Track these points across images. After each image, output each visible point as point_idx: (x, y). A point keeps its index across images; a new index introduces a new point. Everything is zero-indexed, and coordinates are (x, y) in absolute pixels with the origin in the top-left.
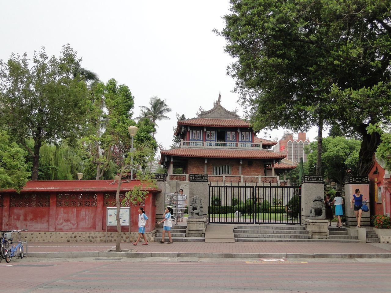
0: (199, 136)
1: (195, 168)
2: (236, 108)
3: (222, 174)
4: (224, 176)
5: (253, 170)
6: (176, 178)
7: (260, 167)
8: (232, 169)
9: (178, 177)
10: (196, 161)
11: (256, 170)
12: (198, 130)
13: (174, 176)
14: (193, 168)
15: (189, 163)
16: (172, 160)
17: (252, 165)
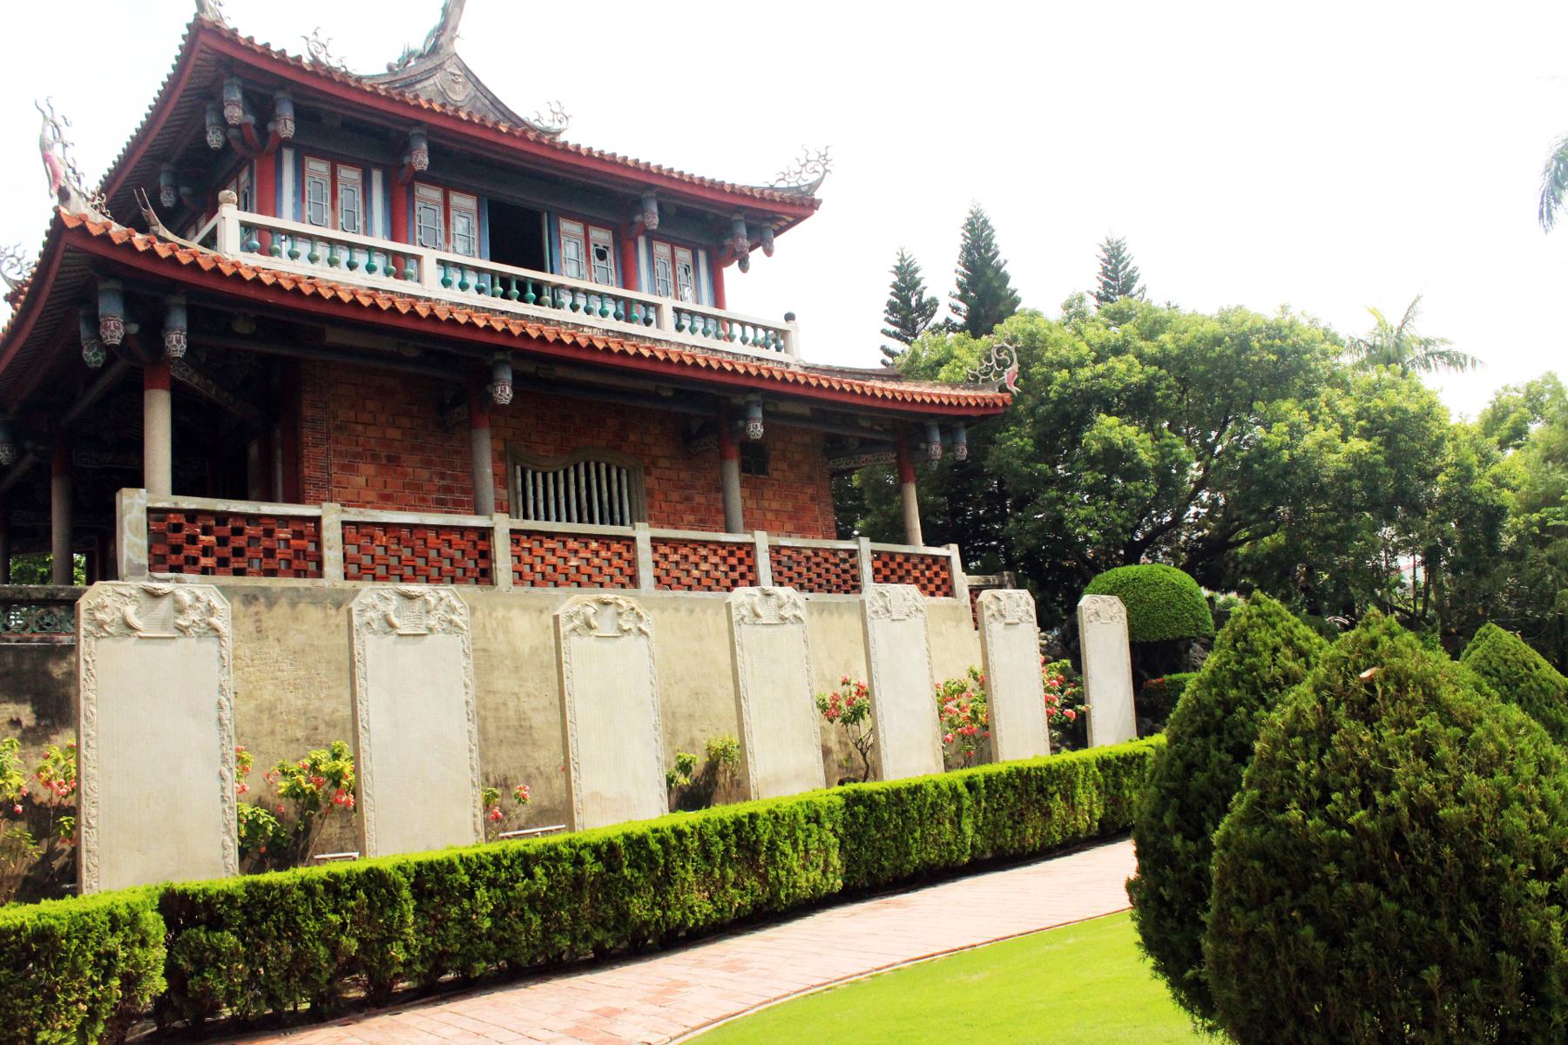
0: (359, 209)
1: (368, 469)
2: (557, 109)
3: (627, 521)
4: (643, 533)
5: (775, 505)
6: (222, 541)
7: (809, 491)
8: (650, 493)
9: (238, 532)
10: (370, 405)
11: (789, 506)
12: (352, 163)
13: (192, 515)
14: (350, 468)
15: (307, 412)
16: (177, 343)
17: (764, 472)
